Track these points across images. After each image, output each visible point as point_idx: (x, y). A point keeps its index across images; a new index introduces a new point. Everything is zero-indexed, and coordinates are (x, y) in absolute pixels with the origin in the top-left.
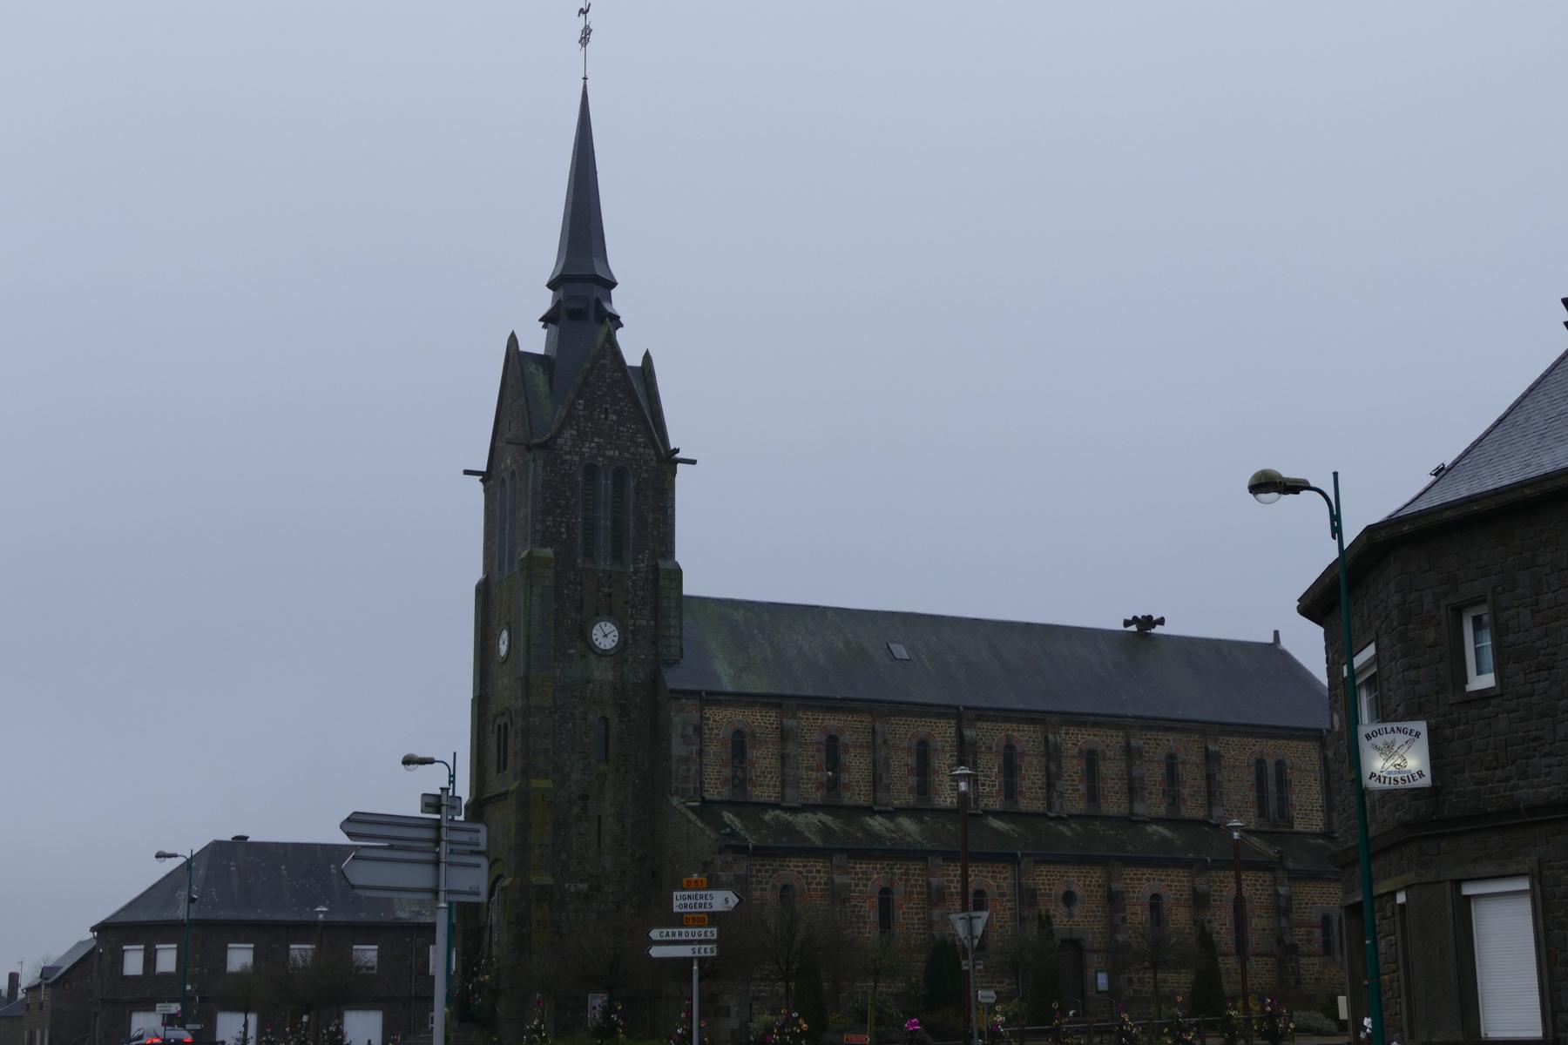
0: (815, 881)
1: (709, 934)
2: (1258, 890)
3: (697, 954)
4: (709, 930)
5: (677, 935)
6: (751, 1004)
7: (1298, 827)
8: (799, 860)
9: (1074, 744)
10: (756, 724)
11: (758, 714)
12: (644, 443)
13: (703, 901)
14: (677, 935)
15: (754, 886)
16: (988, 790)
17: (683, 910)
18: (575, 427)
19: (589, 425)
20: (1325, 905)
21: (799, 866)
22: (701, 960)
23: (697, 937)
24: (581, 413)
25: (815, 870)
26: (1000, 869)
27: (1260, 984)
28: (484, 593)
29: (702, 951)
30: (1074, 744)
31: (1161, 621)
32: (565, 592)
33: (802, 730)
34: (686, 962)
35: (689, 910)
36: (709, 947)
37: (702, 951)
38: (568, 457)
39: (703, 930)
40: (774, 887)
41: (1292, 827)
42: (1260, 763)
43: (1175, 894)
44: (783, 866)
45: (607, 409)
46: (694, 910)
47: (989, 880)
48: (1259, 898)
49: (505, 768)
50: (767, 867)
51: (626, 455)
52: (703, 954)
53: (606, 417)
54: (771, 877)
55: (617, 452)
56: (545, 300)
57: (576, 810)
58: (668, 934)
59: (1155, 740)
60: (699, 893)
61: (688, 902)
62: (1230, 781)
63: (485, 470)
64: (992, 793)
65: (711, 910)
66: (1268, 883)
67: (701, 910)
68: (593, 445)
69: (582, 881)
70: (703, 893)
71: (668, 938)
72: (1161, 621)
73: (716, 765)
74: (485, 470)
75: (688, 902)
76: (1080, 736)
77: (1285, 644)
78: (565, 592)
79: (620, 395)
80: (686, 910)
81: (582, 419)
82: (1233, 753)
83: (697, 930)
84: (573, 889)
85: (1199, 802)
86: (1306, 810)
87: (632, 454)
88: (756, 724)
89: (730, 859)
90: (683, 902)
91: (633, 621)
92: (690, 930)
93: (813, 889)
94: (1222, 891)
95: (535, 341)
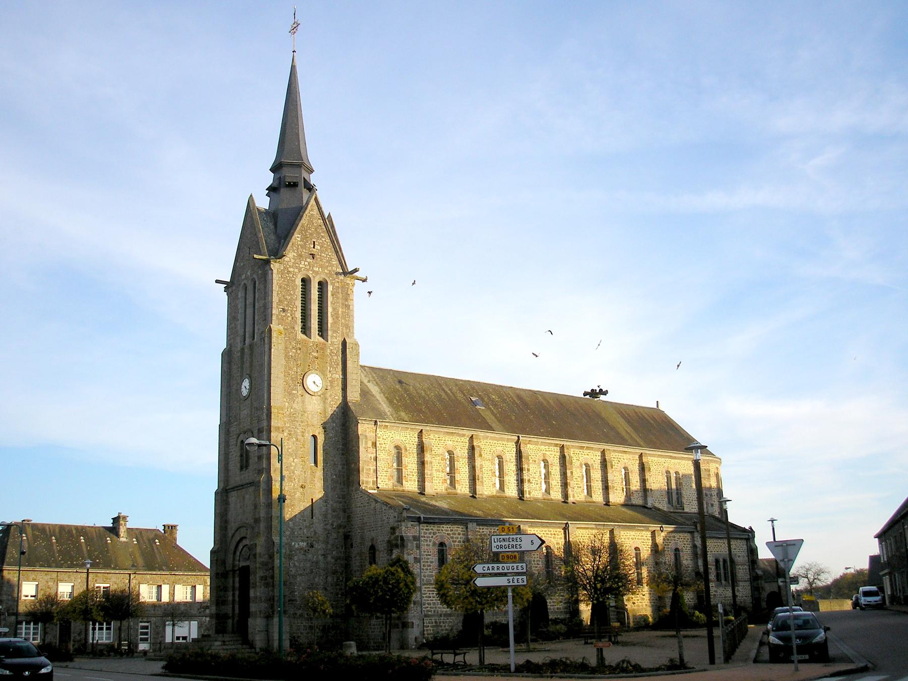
0: (457, 541)
1: (519, 568)
2: (685, 544)
3: (511, 584)
4: (520, 565)
5: (496, 569)
6: (423, 619)
7: (686, 510)
8: (448, 527)
9: (578, 460)
10: (406, 442)
11: (408, 436)
12: (336, 264)
13: (514, 543)
14: (496, 569)
15: (422, 543)
16: (534, 486)
17: (499, 550)
18: (296, 251)
19: (304, 250)
20: (716, 553)
21: (448, 531)
22: (515, 589)
23: (510, 571)
24: (299, 243)
25: (457, 533)
26: (558, 532)
27: (688, 599)
28: (227, 356)
29: (515, 581)
30: (578, 460)
31: (605, 393)
32: (291, 354)
33: (433, 446)
34: (502, 590)
35: (504, 550)
36: (520, 577)
37: (515, 581)
38: (291, 270)
39: (515, 565)
40: (434, 544)
41: (683, 509)
42: (668, 472)
43: (646, 547)
44: (439, 530)
45: (314, 242)
46: (507, 550)
47: (552, 539)
48: (686, 549)
49: (247, 467)
50: (430, 531)
51: (326, 271)
52: (516, 584)
53: (314, 247)
54: (432, 537)
55: (320, 269)
56: (269, 179)
57: (298, 494)
58: (488, 569)
59: (617, 458)
60: (511, 537)
61: (503, 543)
62: (654, 483)
63: (229, 281)
64: (536, 488)
65: (520, 550)
66: (690, 540)
67: (513, 550)
68: (306, 263)
69: (303, 541)
70: (515, 537)
71: (488, 571)
72: (605, 393)
73: (385, 467)
74: (229, 281)
75: (503, 543)
76: (580, 455)
77: (661, 408)
78: (291, 354)
79: (322, 234)
80: (502, 550)
81: (300, 247)
82: (655, 467)
83: (511, 565)
84: (297, 546)
85: (640, 495)
86: (689, 500)
87: (330, 271)
88: (406, 442)
89: (409, 525)
90: (499, 544)
91: (331, 375)
92: (505, 565)
93: (457, 545)
94: (668, 545)
95: (263, 202)
